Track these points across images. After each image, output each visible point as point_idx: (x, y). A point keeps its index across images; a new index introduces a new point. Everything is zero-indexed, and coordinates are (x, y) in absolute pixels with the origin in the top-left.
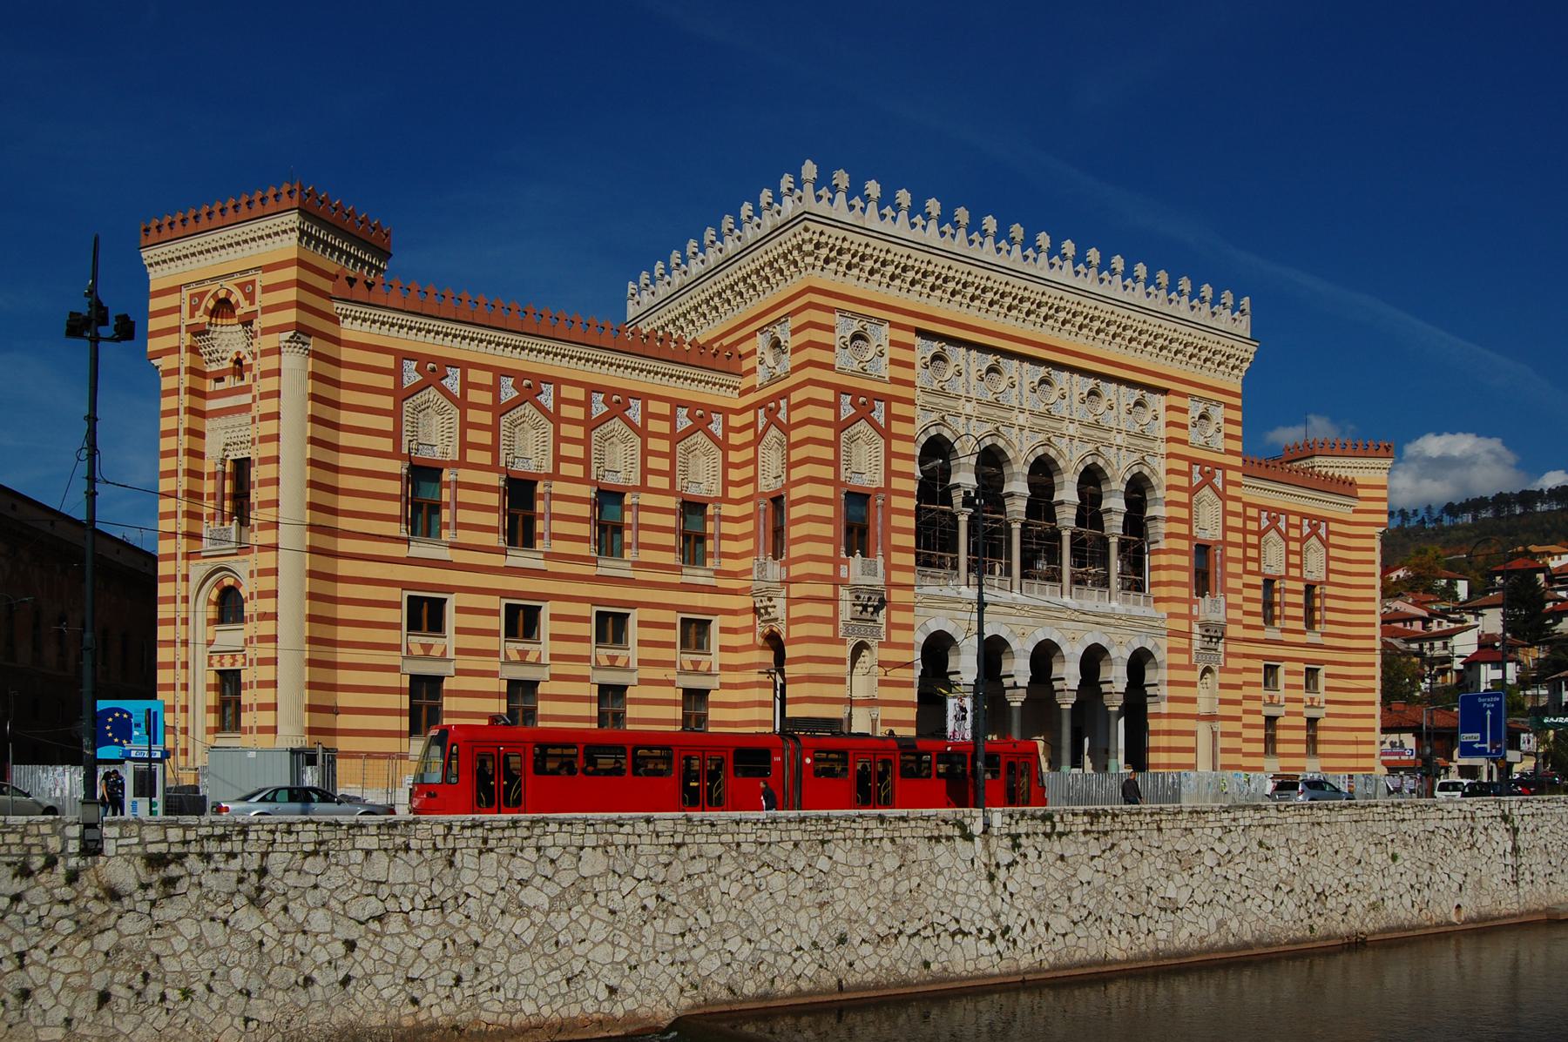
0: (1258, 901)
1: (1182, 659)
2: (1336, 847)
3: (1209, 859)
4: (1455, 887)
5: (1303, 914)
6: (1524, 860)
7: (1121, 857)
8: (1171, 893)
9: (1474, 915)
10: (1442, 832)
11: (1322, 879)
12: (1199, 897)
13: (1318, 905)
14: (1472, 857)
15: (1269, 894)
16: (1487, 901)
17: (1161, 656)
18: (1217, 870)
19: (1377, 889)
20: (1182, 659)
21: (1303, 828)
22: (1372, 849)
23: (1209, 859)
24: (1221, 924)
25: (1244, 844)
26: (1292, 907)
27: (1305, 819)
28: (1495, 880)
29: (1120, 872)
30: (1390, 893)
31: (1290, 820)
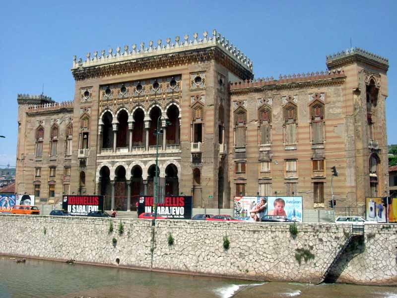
0: (40, 244)
2: (69, 231)
3: (29, 230)
4: (118, 251)
5: (54, 250)
7: (7, 227)
8: (17, 238)
9: (125, 263)
11: (62, 240)
12: (25, 241)
13: (59, 248)
14: (128, 241)
15: (44, 243)
16: (133, 259)
18: (30, 233)
19: (82, 246)
21: (59, 224)
22: (83, 233)
23: (29, 230)
24: (29, 248)
25: (39, 226)
26: (51, 247)
27: (60, 221)
28: (139, 252)
29: (6, 230)
30: (87, 249)
31: (55, 221)
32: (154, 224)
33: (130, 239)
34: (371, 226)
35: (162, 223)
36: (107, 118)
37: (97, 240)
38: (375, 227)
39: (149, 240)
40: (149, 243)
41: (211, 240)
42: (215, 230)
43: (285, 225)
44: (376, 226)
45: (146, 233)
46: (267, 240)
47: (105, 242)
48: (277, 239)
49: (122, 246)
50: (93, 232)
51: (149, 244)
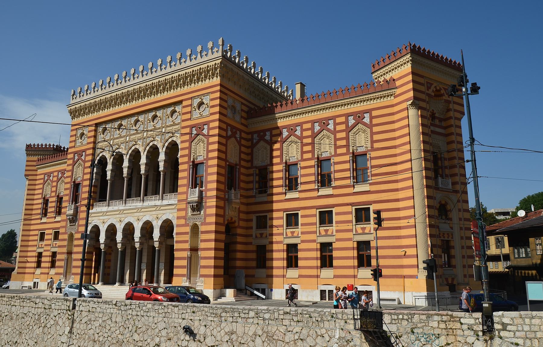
1: (183, 222)
6: (75, 342)
10: (31, 315)
17: (175, 222)
20: (183, 222)
32: (74, 308)
33: (46, 329)
34: (396, 317)
35: (84, 304)
36: (103, 162)
37: (10, 330)
38: (403, 319)
39: (66, 333)
40: (66, 337)
41: (141, 335)
42: (146, 318)
43: (247, 312)
44: (406, 317)
45: (64, 319)
46: (219, 338)
47: (17, 332)
48: (234, 337)
49: (35, 341)
50: (8, 317)
51: (64, 339)
